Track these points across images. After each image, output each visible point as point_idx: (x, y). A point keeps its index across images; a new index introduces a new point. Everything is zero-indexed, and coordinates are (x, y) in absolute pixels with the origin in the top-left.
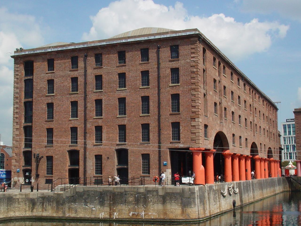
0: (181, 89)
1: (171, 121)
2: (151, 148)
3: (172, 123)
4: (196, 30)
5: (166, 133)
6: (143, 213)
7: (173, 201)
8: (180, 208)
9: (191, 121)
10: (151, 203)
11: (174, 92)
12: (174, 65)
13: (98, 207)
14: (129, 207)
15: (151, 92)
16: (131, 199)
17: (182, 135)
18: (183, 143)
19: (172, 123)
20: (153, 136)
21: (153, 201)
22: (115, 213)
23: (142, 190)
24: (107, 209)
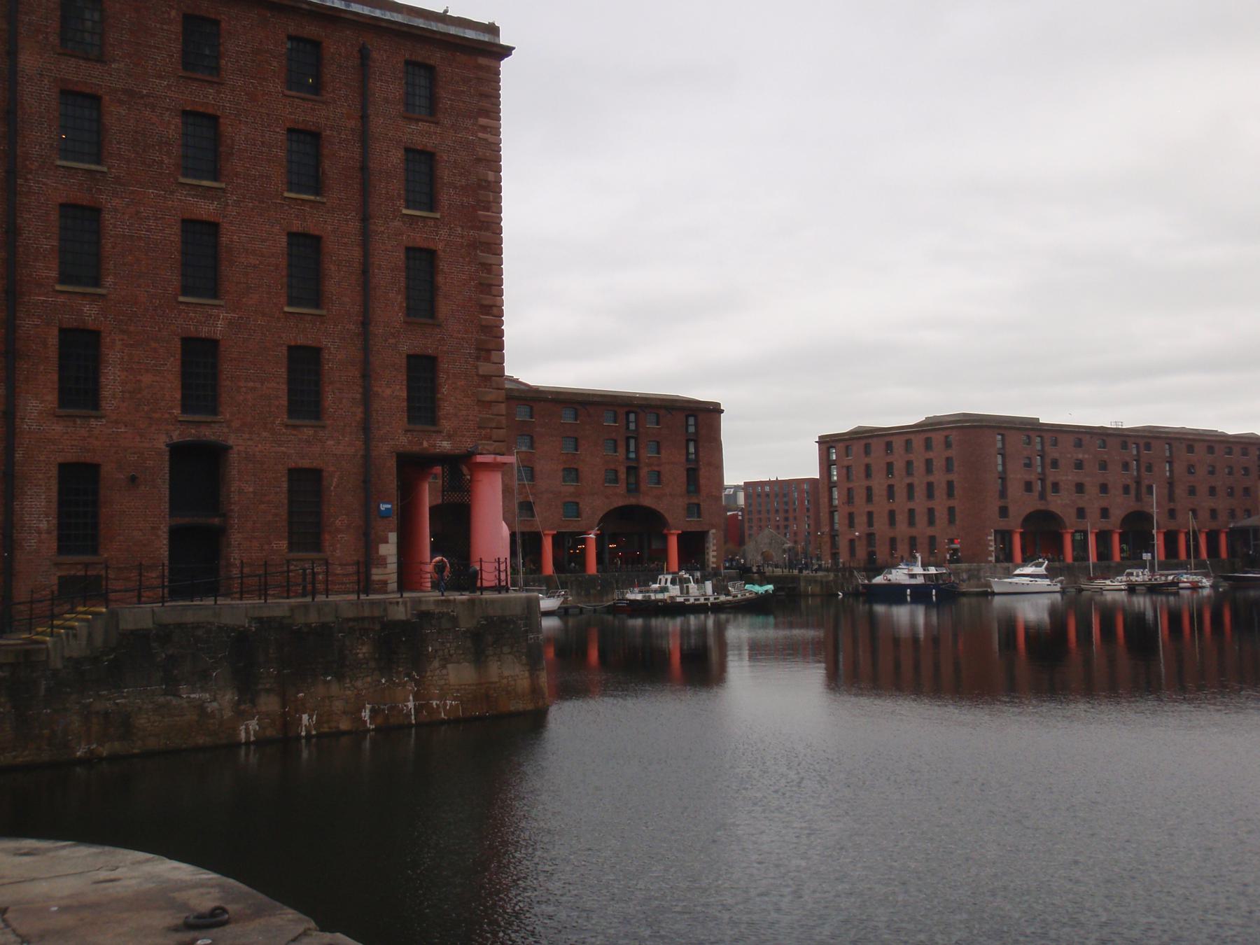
0: (444, 232)
1: (406, 348)
2: (333, 447)
3: (409, 357)
4: (493, 29)
5: (388, 391)
6: (411, 705)
7: (506, 649)
8: (527, 674)
9: (478, 358)
10: (436, 664)
11: (418, 238)
12: (419, 134)
13: (228, 697)
14: (359, 684)
15: (334, 223)
16: (363, 651)
17: (446, 408)
18: (449, 437)
19: (409, 357)
20: (339, 397)
21: (440, 653)
22: (305, 717)
23: (400, 613)
24: (269, 703)
